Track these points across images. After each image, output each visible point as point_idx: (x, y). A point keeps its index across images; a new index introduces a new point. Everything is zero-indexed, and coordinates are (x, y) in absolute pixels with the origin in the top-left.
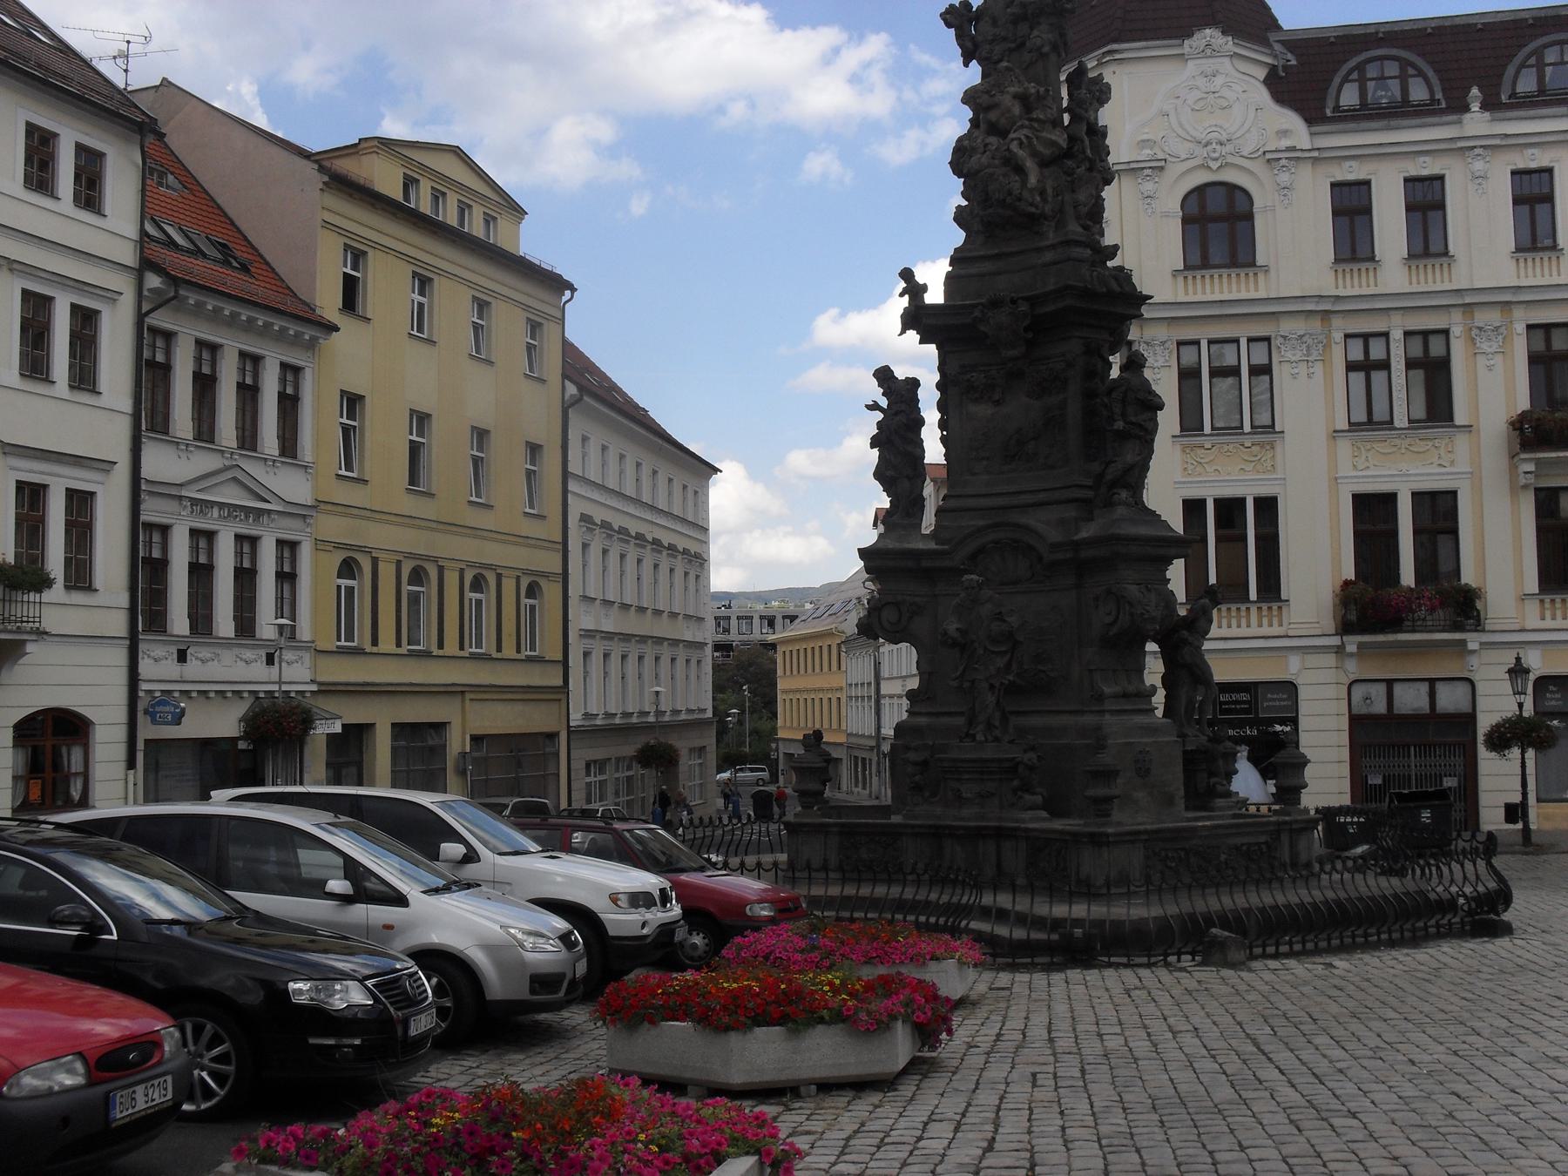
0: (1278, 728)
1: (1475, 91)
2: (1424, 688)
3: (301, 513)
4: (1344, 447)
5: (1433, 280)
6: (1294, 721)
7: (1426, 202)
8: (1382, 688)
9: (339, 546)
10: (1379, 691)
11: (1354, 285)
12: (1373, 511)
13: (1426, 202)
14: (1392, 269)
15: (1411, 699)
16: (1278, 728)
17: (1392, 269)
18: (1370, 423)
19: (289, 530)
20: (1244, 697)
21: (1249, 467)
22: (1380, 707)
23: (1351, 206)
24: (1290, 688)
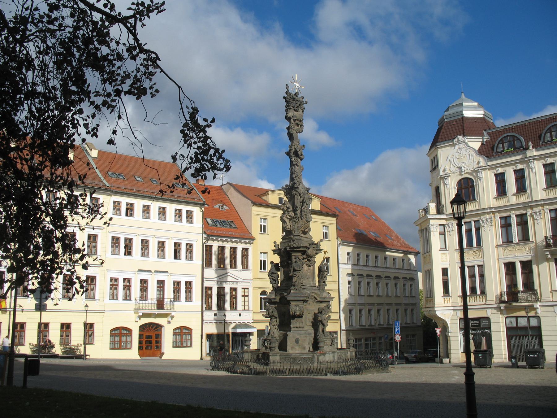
0: (486, 331)
1: (530, 143)
2: (526, 319)
3: (249, 281)
4: (501, 249)
5: (524, 199)
6: (489, 328)
7: (520, 176)
8: (515, 319)
9: (260, 288)
10: (514, 320)
11: (503, 202)
12: (510, 267)
13: (520, 176)
14: (512, 199)
15: (523, 322)
16: (486, 331)
17: (512, 199)
18: (508, 241)
19: (245, 285)
20: (477, 322)
21: (475, 257)
22: (515, 325)
23: (501, 180)
24: (488, 319)
